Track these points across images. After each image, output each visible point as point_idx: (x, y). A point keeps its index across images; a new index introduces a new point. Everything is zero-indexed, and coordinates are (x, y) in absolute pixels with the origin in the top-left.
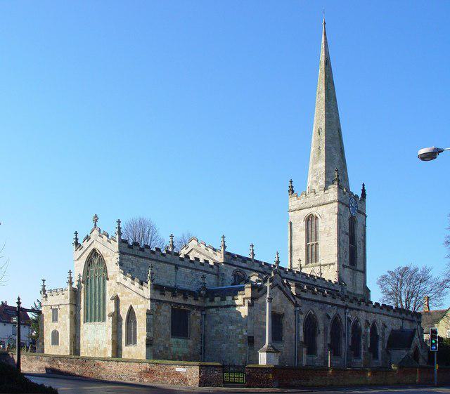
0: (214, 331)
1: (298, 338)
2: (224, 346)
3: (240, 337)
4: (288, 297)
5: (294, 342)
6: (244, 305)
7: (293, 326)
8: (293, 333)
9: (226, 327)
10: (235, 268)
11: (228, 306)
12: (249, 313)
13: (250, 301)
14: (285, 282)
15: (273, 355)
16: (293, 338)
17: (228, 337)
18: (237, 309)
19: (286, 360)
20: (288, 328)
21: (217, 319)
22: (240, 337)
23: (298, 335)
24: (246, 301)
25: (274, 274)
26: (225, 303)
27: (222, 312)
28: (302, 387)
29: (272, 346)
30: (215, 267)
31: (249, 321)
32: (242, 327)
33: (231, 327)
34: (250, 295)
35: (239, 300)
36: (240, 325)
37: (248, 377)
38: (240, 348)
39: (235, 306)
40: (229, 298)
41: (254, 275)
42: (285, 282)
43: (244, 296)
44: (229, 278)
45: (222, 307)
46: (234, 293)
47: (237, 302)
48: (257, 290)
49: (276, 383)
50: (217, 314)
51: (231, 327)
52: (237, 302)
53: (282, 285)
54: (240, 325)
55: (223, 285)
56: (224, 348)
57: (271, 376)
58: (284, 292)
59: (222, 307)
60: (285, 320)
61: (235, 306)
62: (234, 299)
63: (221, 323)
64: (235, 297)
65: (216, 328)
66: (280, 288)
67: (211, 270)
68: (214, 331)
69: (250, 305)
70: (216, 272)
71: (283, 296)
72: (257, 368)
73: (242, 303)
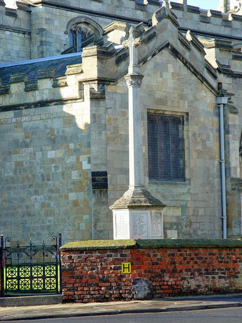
0: (11, 165)
1: (228, 169)
2: (36, 201)
3: (75, 175)
4: (195, 73)
5: (216, 181)
6: (82, 97)
7: (213, 144)
8: (212, 158)
9: (39, 155)
10: (74, 15)
11: (43, 104)
12: (93, 116)
13: (95, 86)
14: (189, 37)
15: (146, 216)
16: (215, 170)
17: (46, 178)
18: (66, 108)
19: (194, 226)
20: (199, 147)
21: (19, 135)
22: (75, 175)
23: (227, 162)
24: (87, 88)
25: (159, 19)
26: (36, 97)
27: (31, 118)
28: (218, 292)
29: (146, 193)
30: (21, 14)
31: (94, 136)
32: (77, 151)
33: (51, 154)
34: (94, 74)
35: (70, 87)
36: (72, 146)
37: (68, 273)
38: (76, 203)
39: (61, 102)
40: (45, 85)
41: (116, 28)
42: (189, 37)
43: (81, 77)
44: (58, 38)
45: (28, 106)
46: (57, 70)
47: (65, 93)
48: (114, 59)
49: (143, 287)
50: (19, 125)
51: (51, 154)
52: (65, 93)
53: (180, 48)
54: (72, 146)
55: (42, 54)
56: (37, 206)
57: (126, 268)
58: (186, 63)
59: (28, 106)
60: (189, 131)
61: (61, 102)
62: (56, 86)
63: (27, 146)
64: (61, 81)
65: (16, 158)
66: (175, 53)
67: (10, 21)
68: (11, 165)
69: (96, 98)
70: (24, 26)
71: (185, 71)
72: (115, 250)
73: (77, 95)
